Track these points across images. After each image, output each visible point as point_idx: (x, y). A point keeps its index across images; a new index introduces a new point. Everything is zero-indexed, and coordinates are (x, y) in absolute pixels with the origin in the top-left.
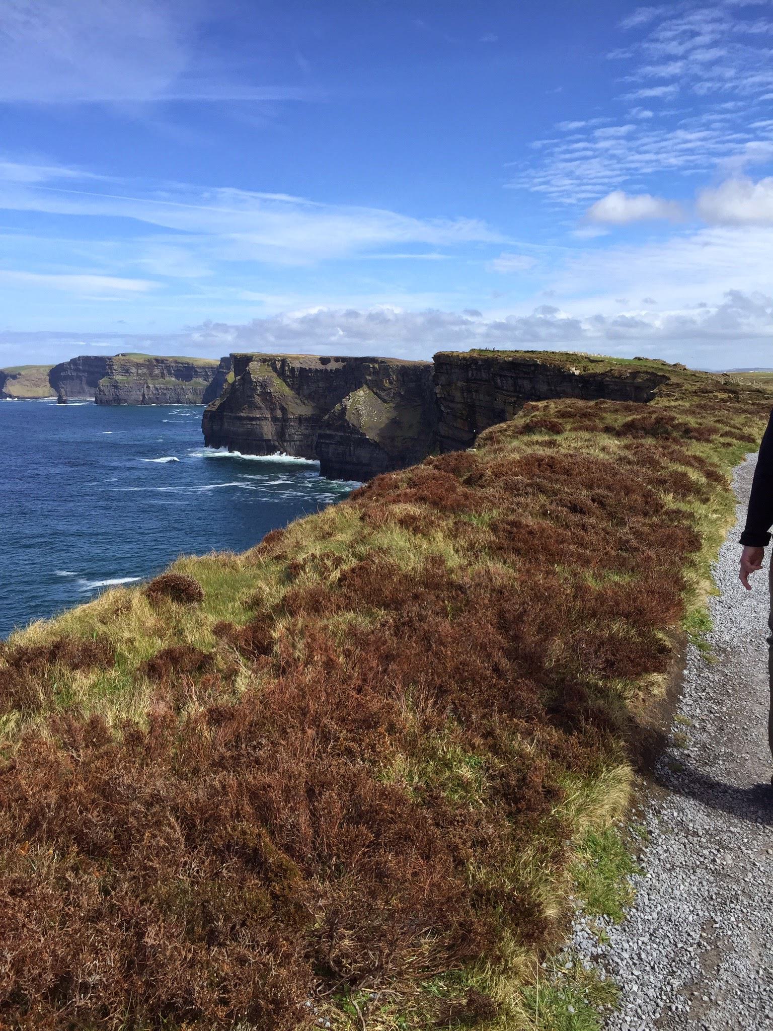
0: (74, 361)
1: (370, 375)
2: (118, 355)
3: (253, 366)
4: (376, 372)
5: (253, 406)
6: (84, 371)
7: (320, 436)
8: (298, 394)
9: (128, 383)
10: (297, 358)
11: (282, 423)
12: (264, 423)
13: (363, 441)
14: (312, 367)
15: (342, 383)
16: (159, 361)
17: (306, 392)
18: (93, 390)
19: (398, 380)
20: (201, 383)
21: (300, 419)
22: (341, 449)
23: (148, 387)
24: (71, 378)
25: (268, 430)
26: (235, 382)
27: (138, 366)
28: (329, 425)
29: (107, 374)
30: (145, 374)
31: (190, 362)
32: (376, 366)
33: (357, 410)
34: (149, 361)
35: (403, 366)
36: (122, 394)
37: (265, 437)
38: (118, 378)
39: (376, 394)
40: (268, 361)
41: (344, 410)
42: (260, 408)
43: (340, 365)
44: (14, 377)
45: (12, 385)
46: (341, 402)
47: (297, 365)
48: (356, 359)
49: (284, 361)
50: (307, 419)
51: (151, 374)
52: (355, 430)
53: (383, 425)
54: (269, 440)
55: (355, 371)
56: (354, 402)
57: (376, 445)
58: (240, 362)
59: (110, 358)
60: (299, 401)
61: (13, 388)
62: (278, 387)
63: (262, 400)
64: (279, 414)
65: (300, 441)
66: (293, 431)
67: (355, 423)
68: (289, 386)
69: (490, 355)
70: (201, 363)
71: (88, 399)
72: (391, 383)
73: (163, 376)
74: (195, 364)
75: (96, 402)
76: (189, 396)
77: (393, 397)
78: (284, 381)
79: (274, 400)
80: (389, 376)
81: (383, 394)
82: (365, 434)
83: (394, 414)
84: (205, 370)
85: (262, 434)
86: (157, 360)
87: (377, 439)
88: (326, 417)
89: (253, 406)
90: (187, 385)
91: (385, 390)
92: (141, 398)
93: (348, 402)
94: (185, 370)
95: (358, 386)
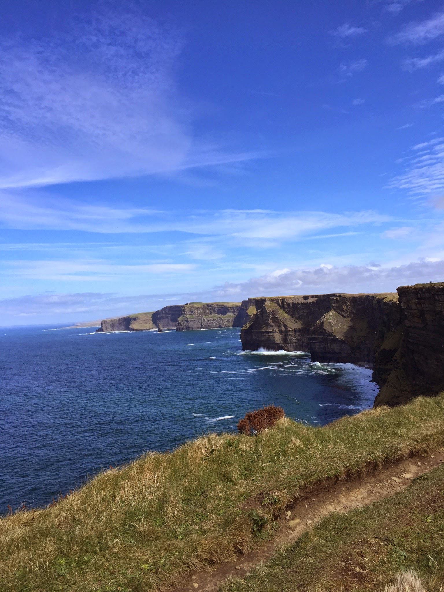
0: (164, 309)
1: (334, 303)
2: (187, 304)
3: (267, 304)
4: (338, 302)
5: (268, 325)
6: (169, 314)
7: (310, 339)
8: (293, 317)
9: (193, 318)
10: (290, 298)
11: (285, 334)
12: (275, 334)
13: (335, 340)
14: (299, 302)
15: (317, 309)
16: (209, 305)
17: (297, 316)
18: (174, 324)
19: (351, 305)
20: (231, 316)
21: (295, 331)
23: (204, 320)
24: (163, 318)
25: (278, 338)
26: (257, 313)
27: (198, 309)
29: (182, 314)
30: (201, 313)
32: (338, 298)
33: (330, 323)
36: (190, 324)
37: (277, 342)
38: (188, 316)
39: (339, 313)
40: (275, 300)
41: (322, 323)
42: (272, 326)
43: (315, 300)
44: (135, 319)
45: (134, 323)
46: (320, 319)
47: (291, 301)
48: (324, 296)
49: (283, 300)
50: (299, 331)
51: (205, 313)
52: (329, 334)
53: (345, 331)
54: (279, 344)
55: (326, 302)
57: (342, 342)
58: (259, 303)
59: (183, 306)
60: (293, 321)
61: (134, 326)
62: (282, 314)
63: (273, 322)
64: (283, 329)
65: (296, 343)
66: (291, 338)
68: (287, 313)
69: (429, 286)
70: (231, 305)
71: (172, 328)
72: (347, 307)
73: (211, 314)
74: (228, 305)
75: (177, 330)
76: (226, 323)
77: (349, 315)
78: (284, 310)
81: (343, 313)
82: (335, 336)
83: (351, 324)
84: (234, 309)
85: (274, 340)
86: (207, 305)
87: (343, 338)
89: (268, 325)
90: (224, 317)
92: (200, 326)
93: (324, 319)
94: (223, 310)
95: (328, 310)
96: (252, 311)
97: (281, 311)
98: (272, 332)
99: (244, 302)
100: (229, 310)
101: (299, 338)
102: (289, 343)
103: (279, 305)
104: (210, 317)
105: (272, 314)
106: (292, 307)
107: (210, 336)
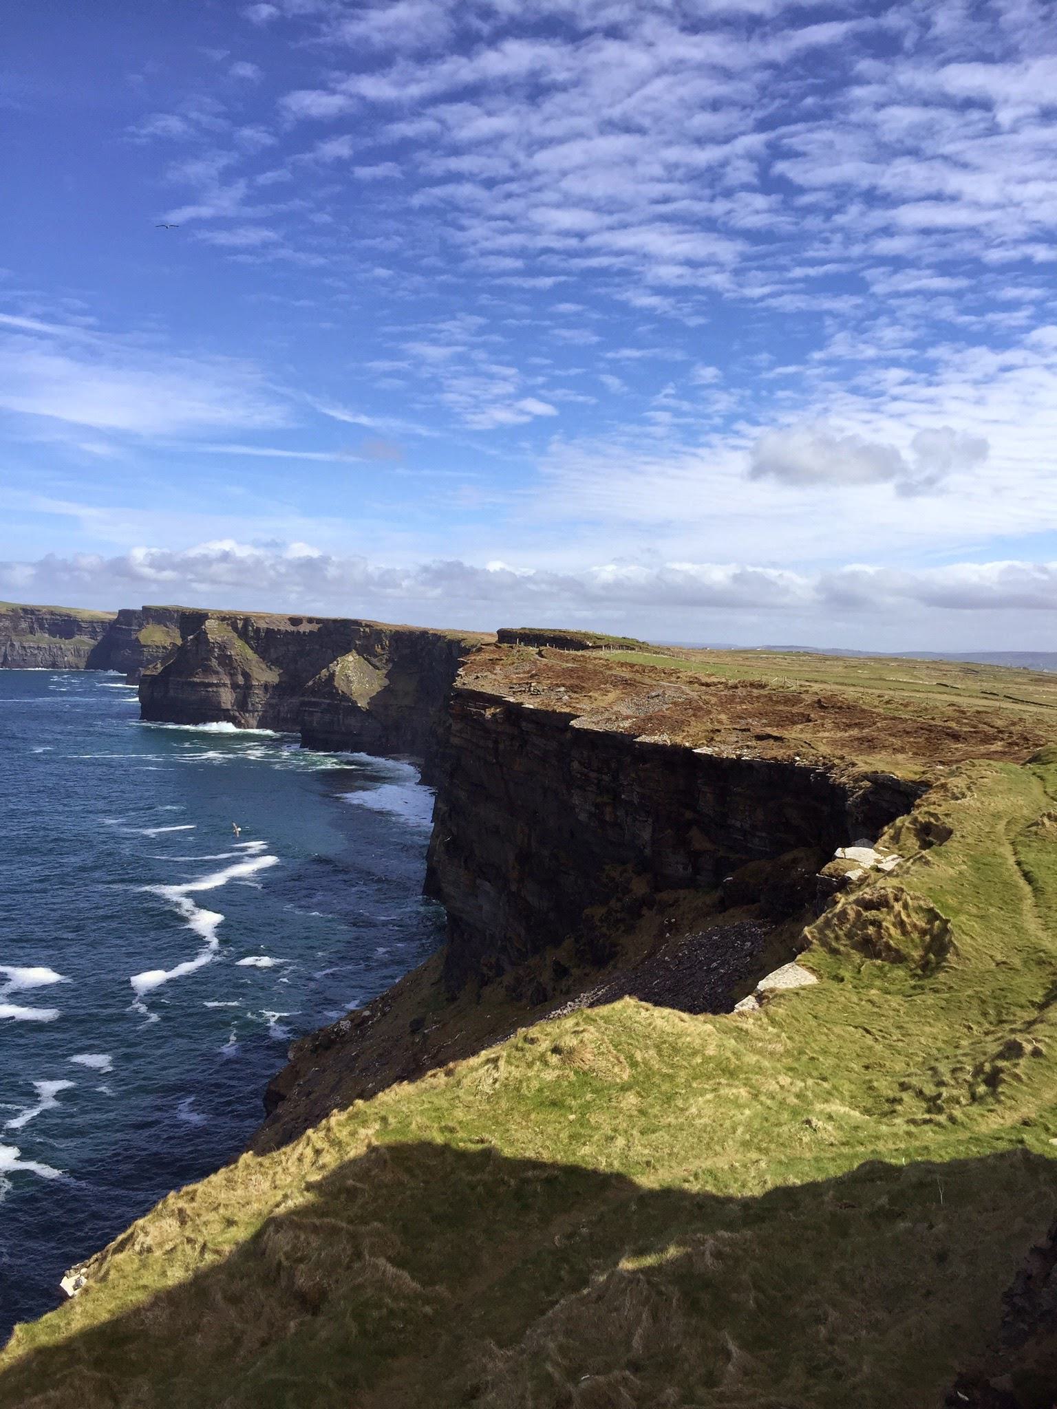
3: (210, 624)
4: (366, 636)
5: (208, 670)
7: (303, 704)
8: (263, 658)
11: (244, 692)
12: (222, 690)
13: (354, 708)
14: (282, 628)
16: (28, 611)
17: (274, 656)
20: (85, 642)
21: (266, 687)
22: (327, 717)
23: (12, 645)
25: (227, 698)
28: (313, 692)
31: (73, 614)
33: (347, 676)
34: (13, 610)
35: (397, 632)
37: (224, 706)
40: (228, 620)
41: (332, 676)
42: (217, 673)
43: (314, 627)
47: (263, 625)
48: (335, 621)
49: (247, 620)
50: (276, 687)
51: (15, 629)
52: (345, 697)
55: (340, 635)
56: (343, 667)
58: (191, 621)
60: (264, 666)
62: (240, 650)
63: (219, 664)
64: (241, 680)
67: (345, 690)
68: (252, 648)
70: (85, 616)
72: (383, 649)
73: (32, 631)
74: (79, 617)
76: (70, 658)
78: (247, 643)
79: (235, 665)
80: (380, 641)
83: (387, 682)
84: (94, 626)
86: (25, 610)
88: (311, 683)
89: (208, 670)
90: (67, 644)
91: (376, 656)
93: (337, 668)
94: (64, 625)
96: (157, 637)
97: (239, 643)
98: (217, 685)
99: (123, 613)
100: (80, 629)
101: (274, 701)
102: (248, 711)
103: (235, 629)
104: (30, 641)
105: (220, 648)
106: (267, 639)
107: (39, 685)
